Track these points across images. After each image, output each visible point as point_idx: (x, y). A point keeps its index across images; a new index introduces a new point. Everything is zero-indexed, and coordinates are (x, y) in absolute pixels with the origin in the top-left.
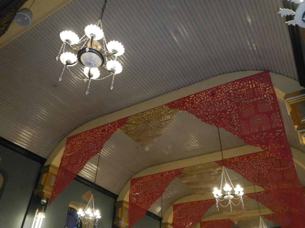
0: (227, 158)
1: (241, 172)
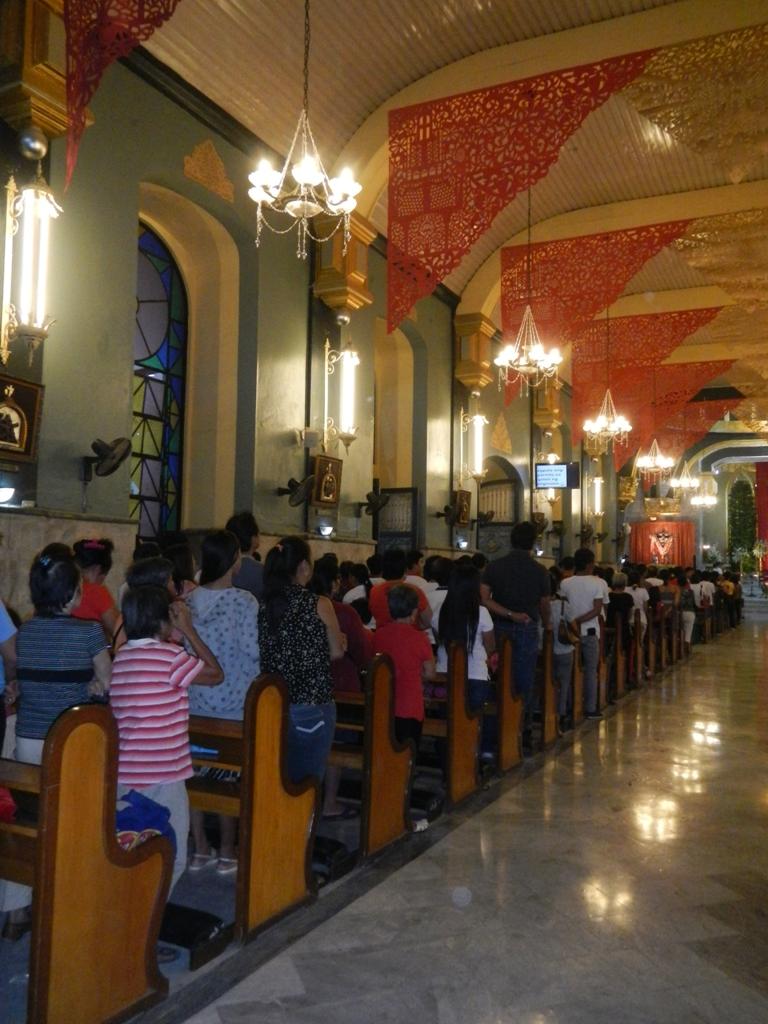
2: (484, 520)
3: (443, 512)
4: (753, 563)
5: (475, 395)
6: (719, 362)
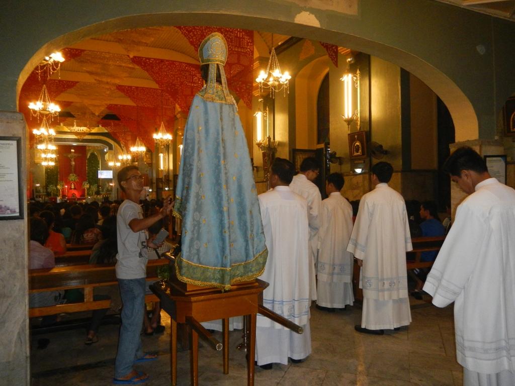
0: (143, 56)
4: (57, 192)
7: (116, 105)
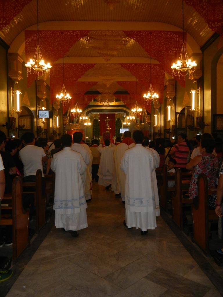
1: (144, 45)
2: (21, 128)
3: (5, 124)
5: (16, 83)
6: (93, 82)
7: (125, 82)
